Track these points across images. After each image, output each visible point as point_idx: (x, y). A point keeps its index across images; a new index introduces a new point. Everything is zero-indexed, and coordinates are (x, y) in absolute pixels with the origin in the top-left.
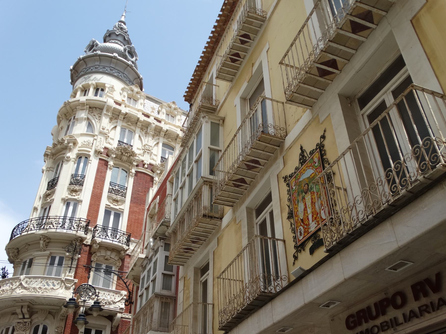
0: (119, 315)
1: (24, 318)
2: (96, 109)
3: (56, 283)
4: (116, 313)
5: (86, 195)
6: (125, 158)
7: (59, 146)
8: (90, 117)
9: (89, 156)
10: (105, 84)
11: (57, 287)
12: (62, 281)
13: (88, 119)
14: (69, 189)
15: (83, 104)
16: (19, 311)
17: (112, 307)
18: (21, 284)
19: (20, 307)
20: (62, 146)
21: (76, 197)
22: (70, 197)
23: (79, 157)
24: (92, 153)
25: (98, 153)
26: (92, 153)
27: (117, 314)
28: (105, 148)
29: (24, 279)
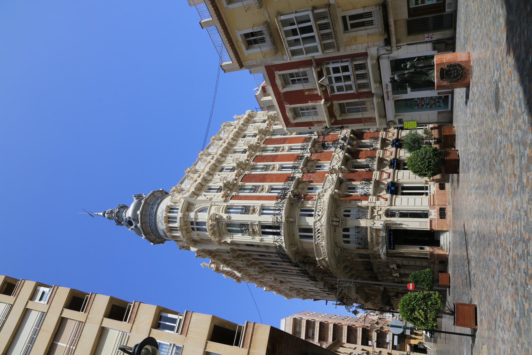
0: (340, 176)
1: (339, 222)
2: (189, 207)
3: (319, 201)
4: (339, 178)
5: (258, 204)
6: (231, 187)
7: (215, 229)
8: (195, 211)
9: (227, 206)
10: (167, 206)
11: (322, 200)
12: (319, 198)
13: (196, 212)
14: (252, 214)
15: (184, 215)
16: (334, 223)
17: (335, 179)
18: (319, 220)
20: (216, 226)
21: (259, 209)
22: (258, 212)
23: (227, 212)
24: (225, 204)
25: (225, 201)
26: (225, 204)
27: (339, 178)
28: (222, 197)
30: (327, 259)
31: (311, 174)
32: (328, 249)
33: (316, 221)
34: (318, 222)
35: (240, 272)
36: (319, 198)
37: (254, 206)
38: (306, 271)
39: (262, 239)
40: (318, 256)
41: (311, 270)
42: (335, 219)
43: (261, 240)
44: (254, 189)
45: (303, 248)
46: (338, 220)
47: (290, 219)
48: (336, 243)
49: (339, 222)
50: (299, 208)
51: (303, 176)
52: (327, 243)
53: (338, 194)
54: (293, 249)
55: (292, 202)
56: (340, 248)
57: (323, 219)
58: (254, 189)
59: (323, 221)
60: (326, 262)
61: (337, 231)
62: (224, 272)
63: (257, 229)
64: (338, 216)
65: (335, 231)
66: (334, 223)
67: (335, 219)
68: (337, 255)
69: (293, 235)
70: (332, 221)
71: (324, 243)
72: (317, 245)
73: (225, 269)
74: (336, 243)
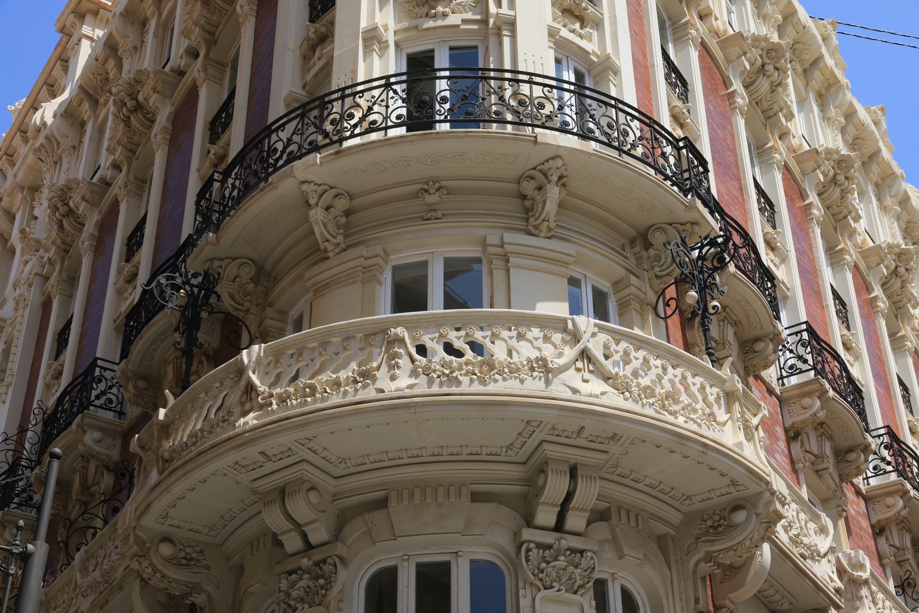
1: (559, 527)
3: (713, 392)
11: (722, 415)
18: (585, 355)
19: (567, 469)
21: (584, 44)
29: (594, 335)
30: (251, 419)
31: (782, 445)
32: (357, 409)
33: (576, 337)
34: (570, 353)
35: (68, 114)
36: (730, 397)
37: (598, 25)
38: (85, 405)
39: (383, 46)
40: (277, 356)
41: (90, 438)
42: (587, 494)
43: (373, 38)
44: (678, 80)
45: (319, 290)
46: (575, 521)
47: (554, 193)
48: (383, 503)
49: (559, 527)
50: (617, 285)
51: (771, 391)
52: (403, 406)
53: (734, 571)
54: (317, 215)
55: (657, 238)
56: (337, 534)
57: (596, 386)
58: (678, 80)
59: (585, 388)
60: (227, 419)
61: (485, 510)
62: (68, 38)
63: (454, 19)
64: (601, 530)
65: (476, 497)
66: (555, 486)
67: (587, 494)
68: (274, 519)
69: (429, 216)
70: (573, 473)
71: (399, 382)
72: (381, 337)
73: (85, 50)
74: (383, 503)
